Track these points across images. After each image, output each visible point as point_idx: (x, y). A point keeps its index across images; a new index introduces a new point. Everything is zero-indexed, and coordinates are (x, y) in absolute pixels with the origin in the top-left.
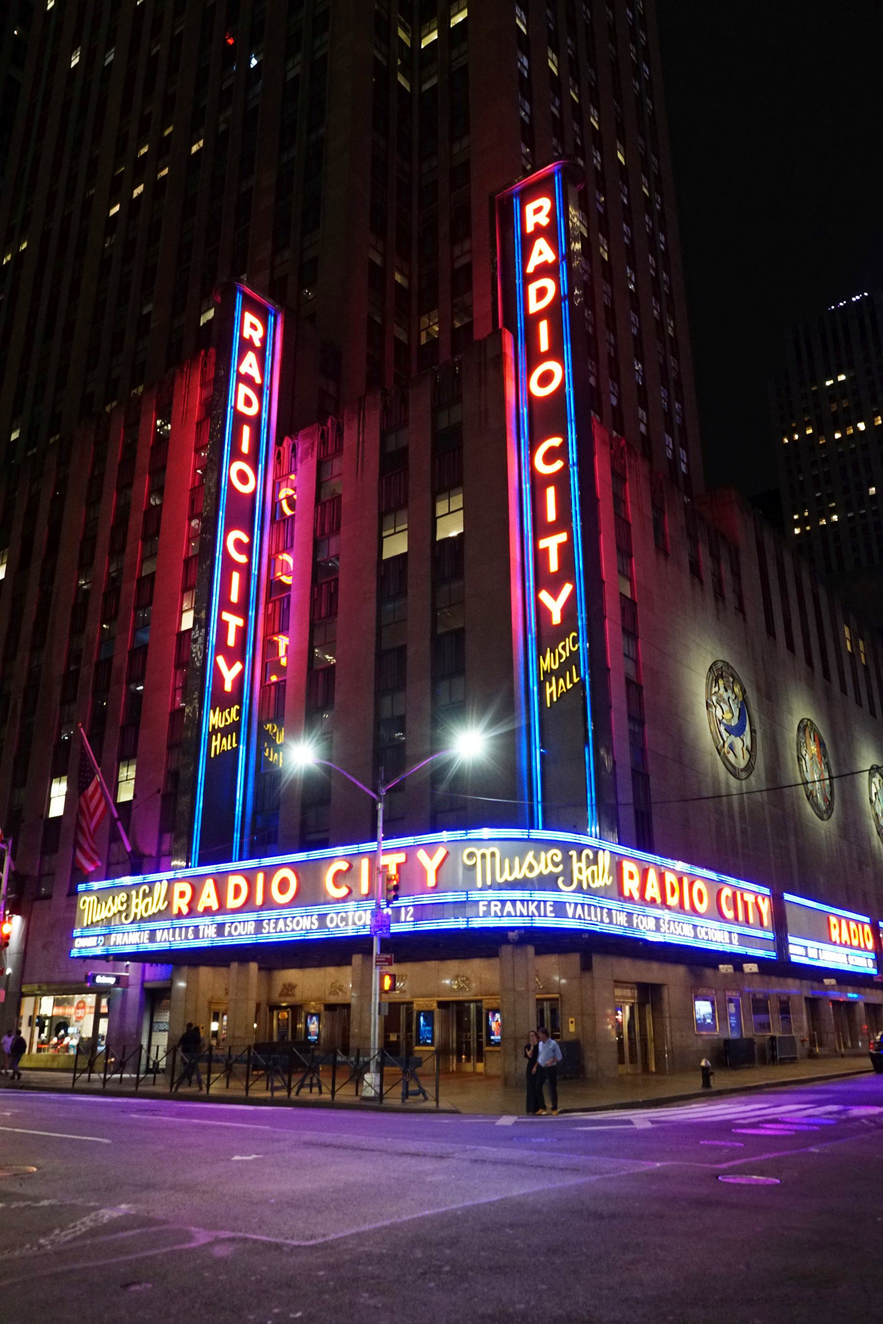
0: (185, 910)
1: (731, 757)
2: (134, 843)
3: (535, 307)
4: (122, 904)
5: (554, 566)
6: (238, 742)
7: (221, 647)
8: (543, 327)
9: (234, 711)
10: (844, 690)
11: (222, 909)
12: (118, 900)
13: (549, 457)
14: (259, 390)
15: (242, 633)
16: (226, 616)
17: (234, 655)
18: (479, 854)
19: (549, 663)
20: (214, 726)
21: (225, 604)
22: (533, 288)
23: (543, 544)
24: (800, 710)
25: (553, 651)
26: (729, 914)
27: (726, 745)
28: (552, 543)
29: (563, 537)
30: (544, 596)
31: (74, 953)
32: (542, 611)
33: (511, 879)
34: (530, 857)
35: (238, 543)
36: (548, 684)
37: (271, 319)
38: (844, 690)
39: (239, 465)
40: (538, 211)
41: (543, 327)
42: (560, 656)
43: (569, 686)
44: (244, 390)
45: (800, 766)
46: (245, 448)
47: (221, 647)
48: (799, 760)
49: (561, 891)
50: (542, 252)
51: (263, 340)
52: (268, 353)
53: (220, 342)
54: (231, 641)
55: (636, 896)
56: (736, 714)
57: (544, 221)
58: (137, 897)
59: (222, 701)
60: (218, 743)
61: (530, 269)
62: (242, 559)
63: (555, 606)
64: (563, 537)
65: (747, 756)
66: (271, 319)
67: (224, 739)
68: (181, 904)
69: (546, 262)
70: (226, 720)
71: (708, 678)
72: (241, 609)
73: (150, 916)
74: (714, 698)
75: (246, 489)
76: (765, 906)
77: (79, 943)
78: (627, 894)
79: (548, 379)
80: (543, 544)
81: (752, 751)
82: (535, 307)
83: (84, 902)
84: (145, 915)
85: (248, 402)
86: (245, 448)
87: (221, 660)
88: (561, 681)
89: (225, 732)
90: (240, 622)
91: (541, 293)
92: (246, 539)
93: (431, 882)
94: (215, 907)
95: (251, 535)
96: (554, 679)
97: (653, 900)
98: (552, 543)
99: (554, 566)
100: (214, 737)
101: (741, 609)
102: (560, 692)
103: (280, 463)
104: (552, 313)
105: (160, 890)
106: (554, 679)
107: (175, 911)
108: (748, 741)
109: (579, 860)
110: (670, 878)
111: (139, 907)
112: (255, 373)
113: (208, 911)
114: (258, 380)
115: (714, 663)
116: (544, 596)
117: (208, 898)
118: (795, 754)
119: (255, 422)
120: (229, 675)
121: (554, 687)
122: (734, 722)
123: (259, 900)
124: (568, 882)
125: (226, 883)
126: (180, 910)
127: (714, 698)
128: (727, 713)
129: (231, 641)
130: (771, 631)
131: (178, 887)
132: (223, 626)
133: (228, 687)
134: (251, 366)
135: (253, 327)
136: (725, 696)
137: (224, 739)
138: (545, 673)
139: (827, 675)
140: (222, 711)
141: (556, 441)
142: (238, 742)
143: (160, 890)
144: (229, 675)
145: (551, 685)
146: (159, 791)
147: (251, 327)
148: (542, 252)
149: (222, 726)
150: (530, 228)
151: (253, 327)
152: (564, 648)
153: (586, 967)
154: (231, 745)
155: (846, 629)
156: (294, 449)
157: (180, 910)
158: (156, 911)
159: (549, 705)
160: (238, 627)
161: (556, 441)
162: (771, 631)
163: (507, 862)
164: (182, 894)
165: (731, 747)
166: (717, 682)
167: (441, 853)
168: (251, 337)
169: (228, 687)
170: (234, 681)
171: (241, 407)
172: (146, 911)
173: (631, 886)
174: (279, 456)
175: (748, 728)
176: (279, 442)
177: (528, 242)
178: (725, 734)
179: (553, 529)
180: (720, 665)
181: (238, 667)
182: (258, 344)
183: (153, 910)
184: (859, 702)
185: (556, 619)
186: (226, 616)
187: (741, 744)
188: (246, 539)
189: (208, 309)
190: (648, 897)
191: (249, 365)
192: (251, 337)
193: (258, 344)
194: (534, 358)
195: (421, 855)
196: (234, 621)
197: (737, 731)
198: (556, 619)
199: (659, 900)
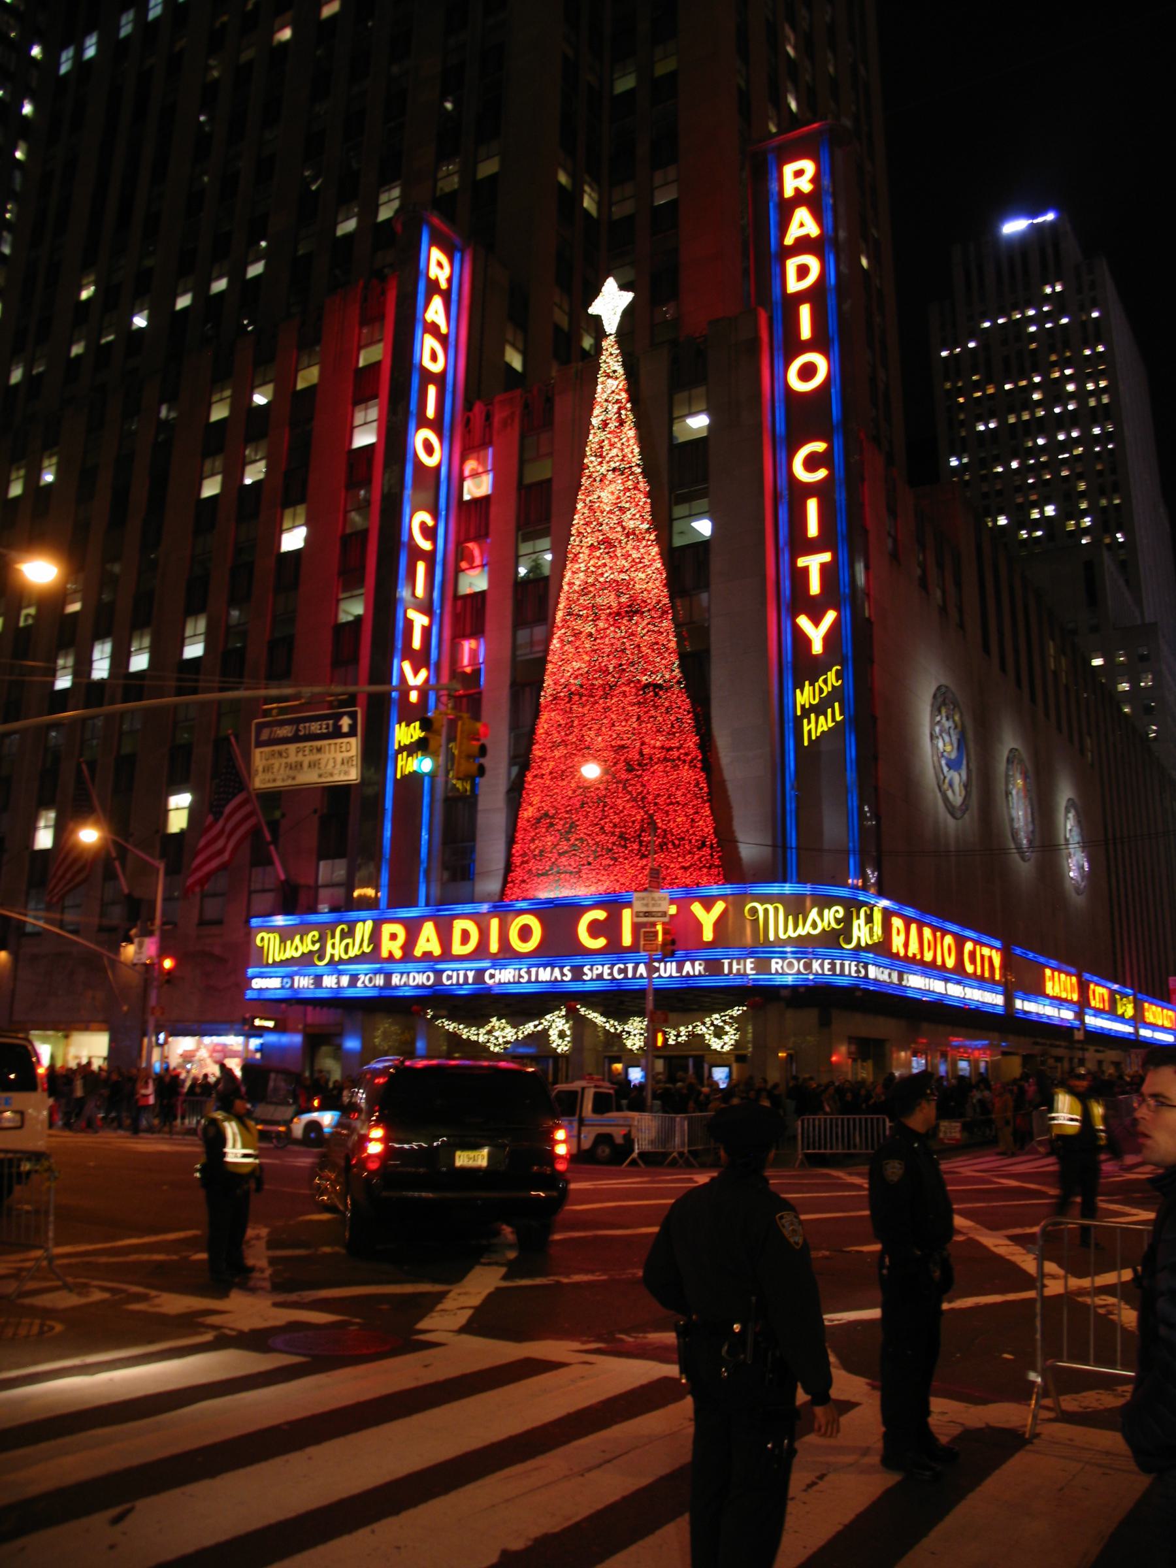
0: (398, 954)
1: (949, 793)
2: (286, 871)
3: (794, 285)
4: (314, 943)
5: (815, 588)
7: (408, 653)
8: (805, 311)
10: (1047, 715)
11: (447, 955)
12: (308, 939)
13: (811, 463)
14: (443, 340)
15: (426, 631)
16: (412, 614)
17: (420, 660)
18: (760, 908)
19: (805, 697)
22: (791, 265)
23: (801, 562)
24: (1009, 742)
25: (812, 684)
26: (970, 968)
27: (947, 781)
28: (814, 563)
29: (826, 557)
30: (803, 621)
31: (250, 994)
32: (802, 640)
33: (794, 935)
34: (814, 914)
35: (423, 525)
36: (805, 721)
37: (458, 256)
38: (1047, 715)
39: (425, 433)
40: (799, 174)
41: (805, 311)
42: (821, 691)
43: (831, 724)
44: (430, 342)
45: (1008, 801)
46: (431, 413)
48: (1007, 796)
49: (842, 948)
50: (803, 224)
51: (449, 280)
52: (454, 296)
53: (412, 288)
54: (416, 644)
55: (902, 953)
56: (955, 745)
57: (806, 187)
58: (333, 937)
61: (789, 241)
62: (426, 545)
63: (816, 634)
64: (826, 557)
65: (963, 793)
66: (458, 256)
68: (391, 947)
69: (808, 236)
71: (932, 705)
73: (350, 958)
74: (937, 729)
75: (430, 462)
76: (997, 961)
77: (257, 983)
78: (894, 951)
79: (809, 373)
80: (801, 562)
81: (966, 786)
82: (794, 285)
83: (262, 939)
84: (345, 957)
85: (434, 358)
86: (431, 413)
87: (407, 666)
88: (822, 718)
91: (803, 271)
92: (430, 523)
93: (708, 935)
94: (437, 951)
95: (436, 517)
96: (813, 716)
97: (914, 955)
98: (814, 563)
99: (815, 588)
100: (400, 756)
101: (961, 626)
102: (820, 730)
103: (469, 432)
104: (811, 295)
105: (364, 929)
106: (813, 716)
107: (385, 954)
108: (964, 777)
109: (858, 918)
110: (927, 932)
111: (336, 948)
113: (427, 956)
114: (444, 330)
115: (939, 688)
116: (803, 621)
117: (428, 940)
118: (1003, 787)
121: (813, 725)
122: (953, 756)
123: (494, 947)
125: (451, 927)
126: (390, 953)
127: (937, 729)
128: (946, 746)
129: (416, 644)
130: (986, 649)
131: (387, 929)
132: (409, 624)
135: (440, 265)
136: (947, 724)
138: (803, 707)
139: (1033, 699)
140: (408, 725)
141: (820, 446)
143: (364, 929)
145: (809, 723)
146: (315, 811)
147: (438, 266)
148: (803, 224)
149: (407, 743)
150: (789, 193)
151: (440, 265)
152: (825, 682)
153: (825, 1022)
155: (1051, 644)
156: (488, 417)
157: (390, 953)
158: (359, 953)
159: (806, 744)
160: (423, 627)
161: (820, 446)
162: (986, 649)
163: (790, 918)
164: (393, 937)
165: (951, 785)
166: (940, 712)
167: (720, 906)
171: (427, 362)
172: (346, 952)
173: (897, 944)
174: (467, 422)
175: (964, 762)
176: (469, 405)
177: (787, 208)
178: (945, 769)
179: (812, 547)
180: (943, 690)
181: (423, 673)
182: (444, 285)
183: (353, 953)
184: (1059, 729)
185: (817, 648)
187: (957, 778)
188: (430, 523)
189: (347, 219)
190: (910, 954)
191: (436, 312)
192: (437, 279)
193: (444, 285)
194: (796, 347)
195: (697, 908)
197: (952, 765)
198: (817, 648)
199: (918, 957)
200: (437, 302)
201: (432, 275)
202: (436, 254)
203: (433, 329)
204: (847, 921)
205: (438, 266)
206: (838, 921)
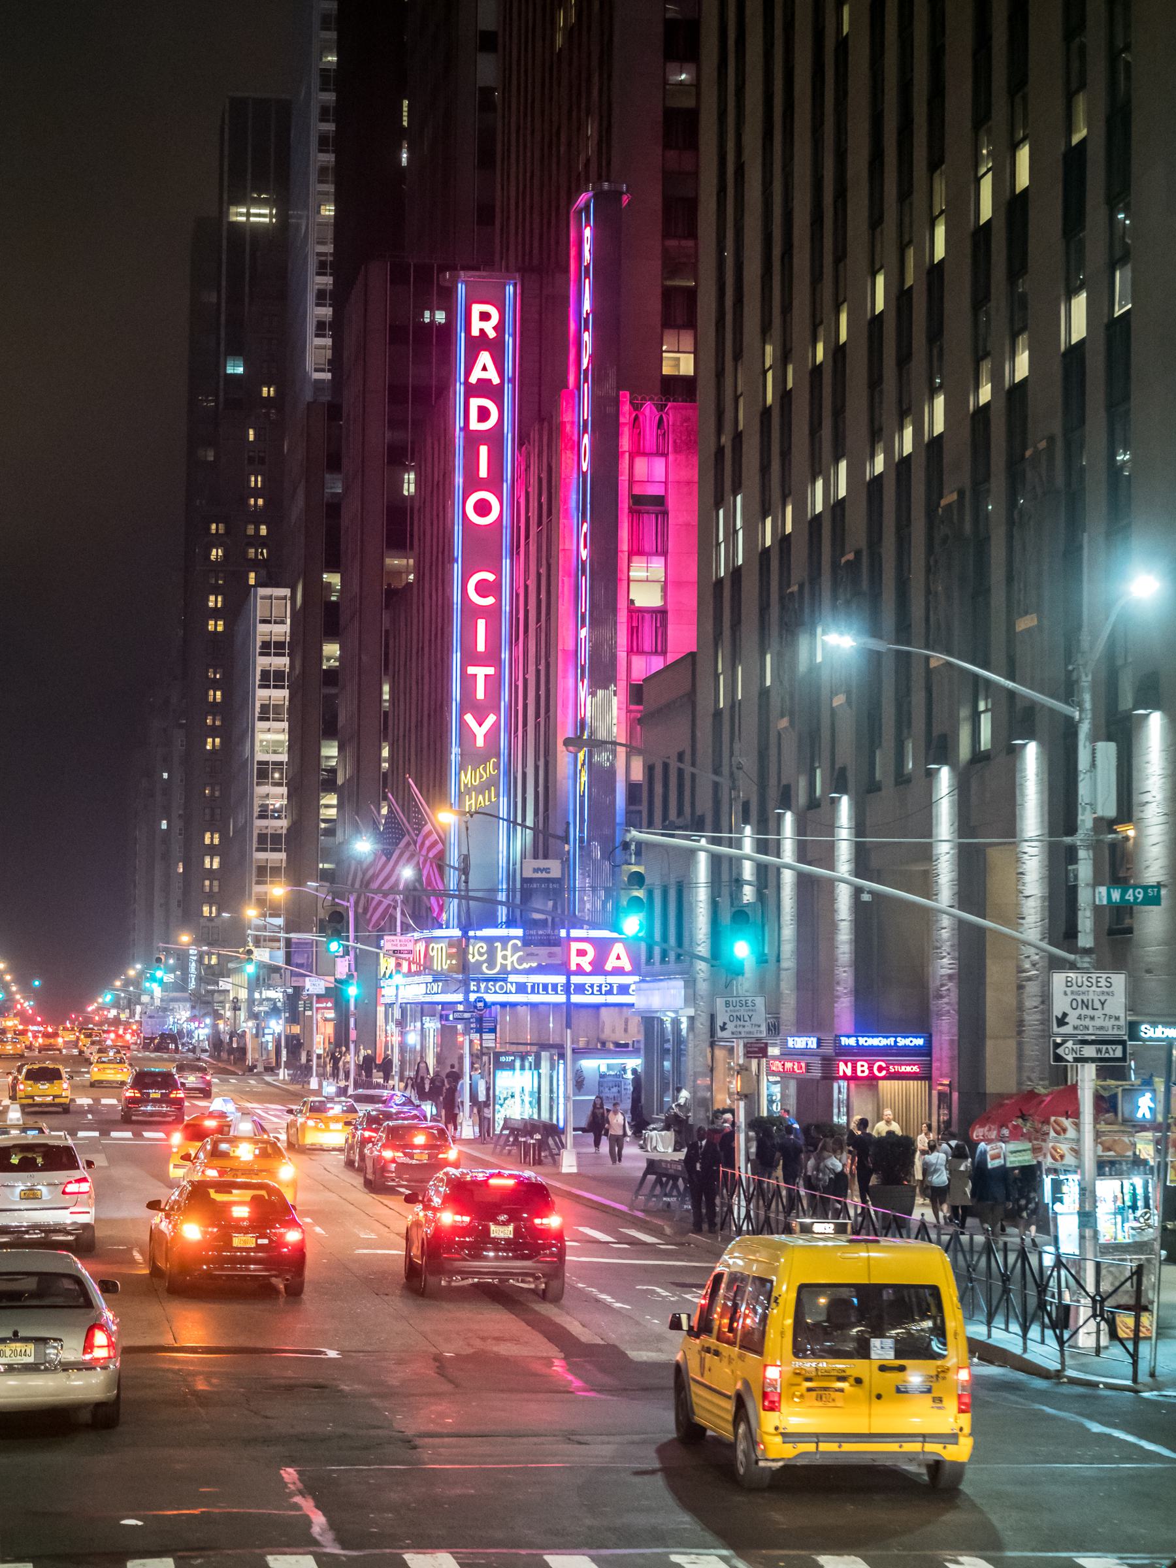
6: (497, 795)
9: (490, 766)
16: (471, 670)
20: (466, 785)
21: (472, 657)
47: (469, 703)
52: (509, 340)
54: (480, 695)
59: (472, 758)
60: (473, 801)
62: (490, 601)
67: (481, 797)
70: (481, 777)
72: (491, 657)
85: (484, 414)
87: (469, 718)
89: (482, 789)
90: (490, 671)
92: (490, 577)
112: (493, 375)
114: (496, 380)
119: (494, 438)
120: (480, 732)
124: (491, 965)
129: (480, 695)
132: (468, 682)
133: (480, 742)
134: (484, 369)
137: (481, 797)
140: (474, 769)
142: (497, 795)
144: (480, 732)
147: (483, 319)
154: (490, 800)
168: (482, 331)
169: (480, 742)
170: (485, 736)
181: (492, 719)
182: (492, 334)
186: (471, 670)
188: (490, 577)
191: (485, 368)
192: (482, 331)
193: (492, 334)
196: (481, 672)
200: (485, 358)
201: (475, 332)
202: (477, 309)
203: (483, 388)
204: (491, 953)
205: (483, 319)
206: (481, 954)
